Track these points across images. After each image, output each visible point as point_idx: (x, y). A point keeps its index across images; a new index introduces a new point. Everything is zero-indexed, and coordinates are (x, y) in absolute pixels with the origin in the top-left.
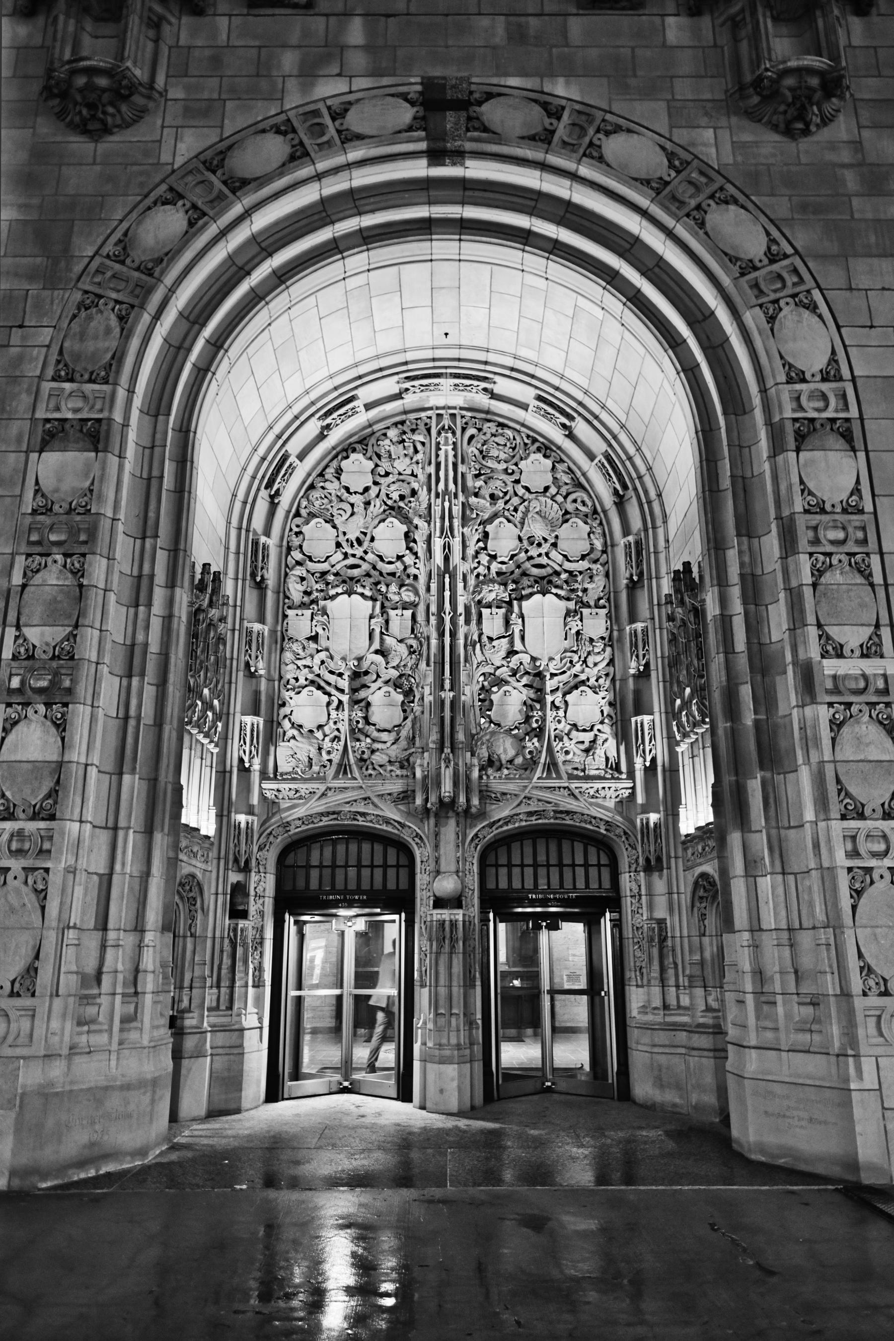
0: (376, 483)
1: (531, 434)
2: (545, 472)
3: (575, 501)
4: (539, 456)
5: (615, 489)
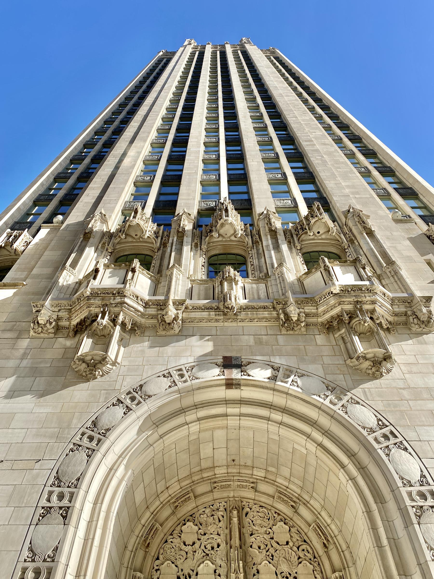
0: (199, 539)
1: (277, 511)
2: (286, 533)
3: (303, 550)
4: (282, 523)
5: (324, 543)
